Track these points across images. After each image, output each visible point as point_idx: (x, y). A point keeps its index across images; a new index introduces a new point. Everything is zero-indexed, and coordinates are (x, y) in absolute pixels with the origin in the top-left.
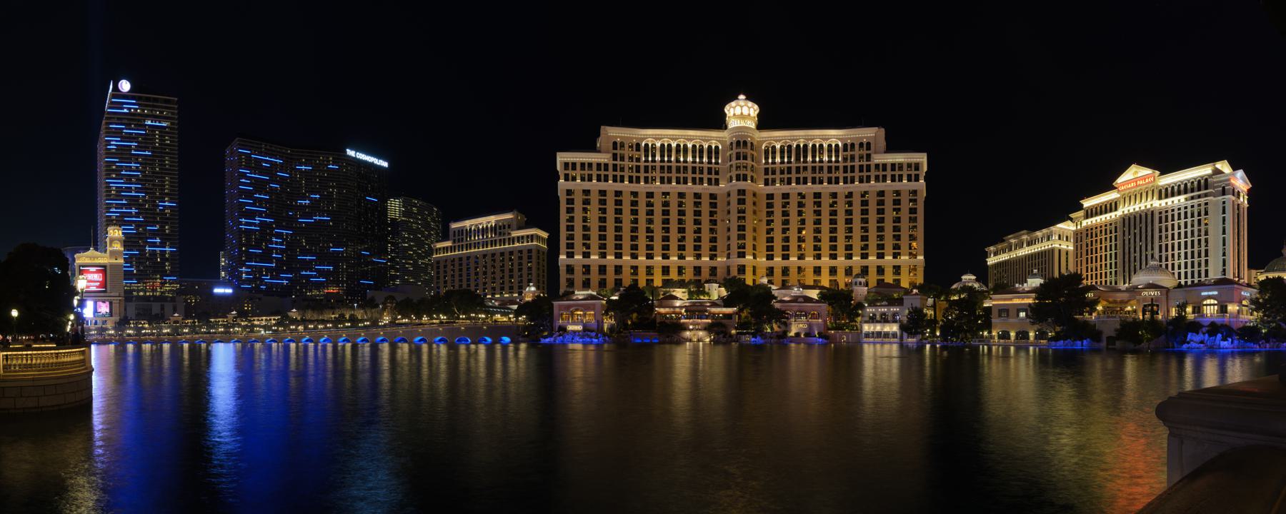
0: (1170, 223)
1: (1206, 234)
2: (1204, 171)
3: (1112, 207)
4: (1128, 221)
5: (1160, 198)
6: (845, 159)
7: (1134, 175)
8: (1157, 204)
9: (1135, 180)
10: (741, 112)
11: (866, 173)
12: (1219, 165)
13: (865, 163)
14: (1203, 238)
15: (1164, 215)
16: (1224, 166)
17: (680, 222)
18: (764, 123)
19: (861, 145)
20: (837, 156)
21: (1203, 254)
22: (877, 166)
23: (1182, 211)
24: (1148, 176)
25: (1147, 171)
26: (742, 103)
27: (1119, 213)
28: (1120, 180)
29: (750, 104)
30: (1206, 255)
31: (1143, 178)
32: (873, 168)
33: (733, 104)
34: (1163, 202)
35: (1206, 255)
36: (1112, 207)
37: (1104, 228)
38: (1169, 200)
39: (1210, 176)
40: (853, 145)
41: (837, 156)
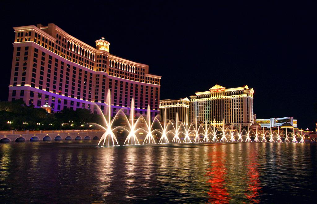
1: (242, 107)
4: (213, 101)
5: (225, 95)
6: (136, 72)
7: (216, 87)
8: (224, 97)
9: (217, 89)
10: (104, 45)
11: (143, 78)
13: (143, 76)
15: (227, 101)
17: (147, 99)
18: (113, 51)
19: (141, 69)
20: (134, 71)
21: (241, 113)
22: (146, 77)
24: (222, 89)
25: (222, 87)
26: (103, 41)
27: (211, 99)
28: (211, 89)
29: (106, 42)
30: (242, 114)
31: (220, 89)
32: (145, 78)
33: (100, 40)
35: (242, 114)
37: (205, 103)
39: (243, 90)
40: (139, 68)
41: (134, 71)
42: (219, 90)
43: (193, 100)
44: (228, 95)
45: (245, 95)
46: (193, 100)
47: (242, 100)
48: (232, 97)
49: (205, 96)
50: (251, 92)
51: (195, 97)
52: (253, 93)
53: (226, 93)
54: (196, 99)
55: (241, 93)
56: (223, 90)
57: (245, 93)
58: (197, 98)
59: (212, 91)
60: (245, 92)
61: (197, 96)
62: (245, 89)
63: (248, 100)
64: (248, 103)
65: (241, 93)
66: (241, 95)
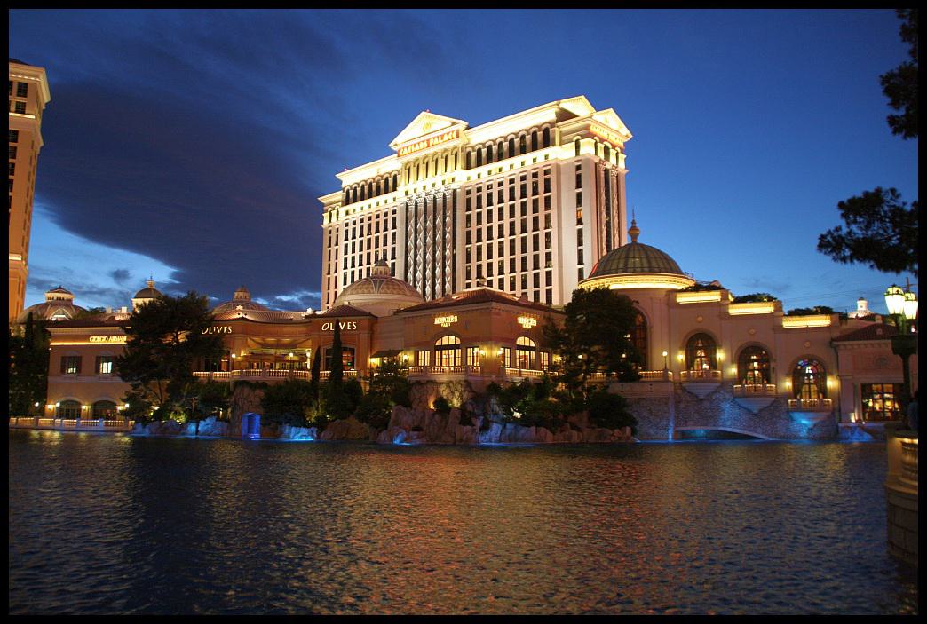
0: (485, 210)
2: (543, 115)
3: (387, 185)
5: (468, 167)
7: (427, 130)
8: (462, 178)
12: (568, 104)
14: (542, 233)
15: (472, 198)
16: (579, 105)
23: (506, 189)
28: (400, 141)
34: (474, 172)
36: (387, 185)
38: (484, 169)
39: (552, 124)
42: (436, 141)
43: (334, 213)
44: (479, 164)
45: (561, 154)
46: (334, 213)
47: (547, 182)
48: (490, 173)
49: (378, 187)
50: (593, 129)
51: (338, 196)
52: (621, 144)
53: (469, 155)
54: (342, 206)
55: (541, 138)
56: (454, 135)
57: (564, 138)
58: (347, 202)
59: (405, 152)
60: (562, 134)
61: (348, 192)
62: (565, 115)
63: (579, 177)
64: (579, 195)
65: (541, 138)
66: (540, 154)
